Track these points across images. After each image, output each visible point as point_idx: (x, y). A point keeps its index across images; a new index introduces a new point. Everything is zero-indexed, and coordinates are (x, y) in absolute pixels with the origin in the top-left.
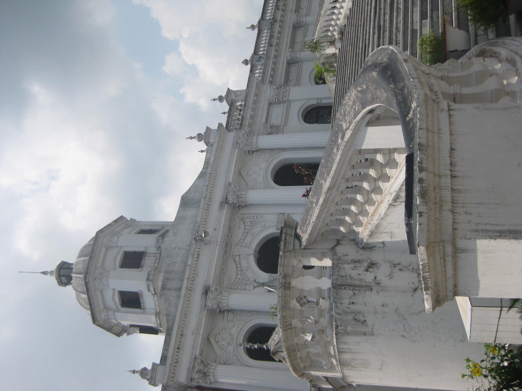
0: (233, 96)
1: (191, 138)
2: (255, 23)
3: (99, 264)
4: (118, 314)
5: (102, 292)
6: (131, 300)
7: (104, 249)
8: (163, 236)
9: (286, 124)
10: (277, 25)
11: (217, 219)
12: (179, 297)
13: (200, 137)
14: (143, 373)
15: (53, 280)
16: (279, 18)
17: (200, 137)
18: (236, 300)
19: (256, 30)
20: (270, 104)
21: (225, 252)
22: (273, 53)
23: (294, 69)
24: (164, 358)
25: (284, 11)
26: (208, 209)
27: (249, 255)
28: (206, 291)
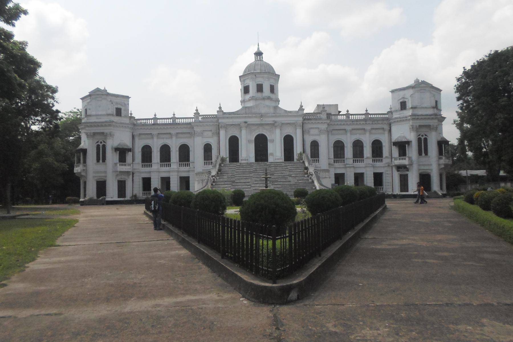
8: (269, 98)
10: (364, 122)
11: (270, 120)
12: (244, 114)
13: (302, 106)
14: (220, 108)
15: (255, 50)
16: (367, 122)
17: (301, 106)
18: (244, 132)
19: (364, 112)
21: (260, 124)
22: (349, 123)
24: (225, 113)
25: (372, 123)
26: (272, 117)
28: (246, 122)
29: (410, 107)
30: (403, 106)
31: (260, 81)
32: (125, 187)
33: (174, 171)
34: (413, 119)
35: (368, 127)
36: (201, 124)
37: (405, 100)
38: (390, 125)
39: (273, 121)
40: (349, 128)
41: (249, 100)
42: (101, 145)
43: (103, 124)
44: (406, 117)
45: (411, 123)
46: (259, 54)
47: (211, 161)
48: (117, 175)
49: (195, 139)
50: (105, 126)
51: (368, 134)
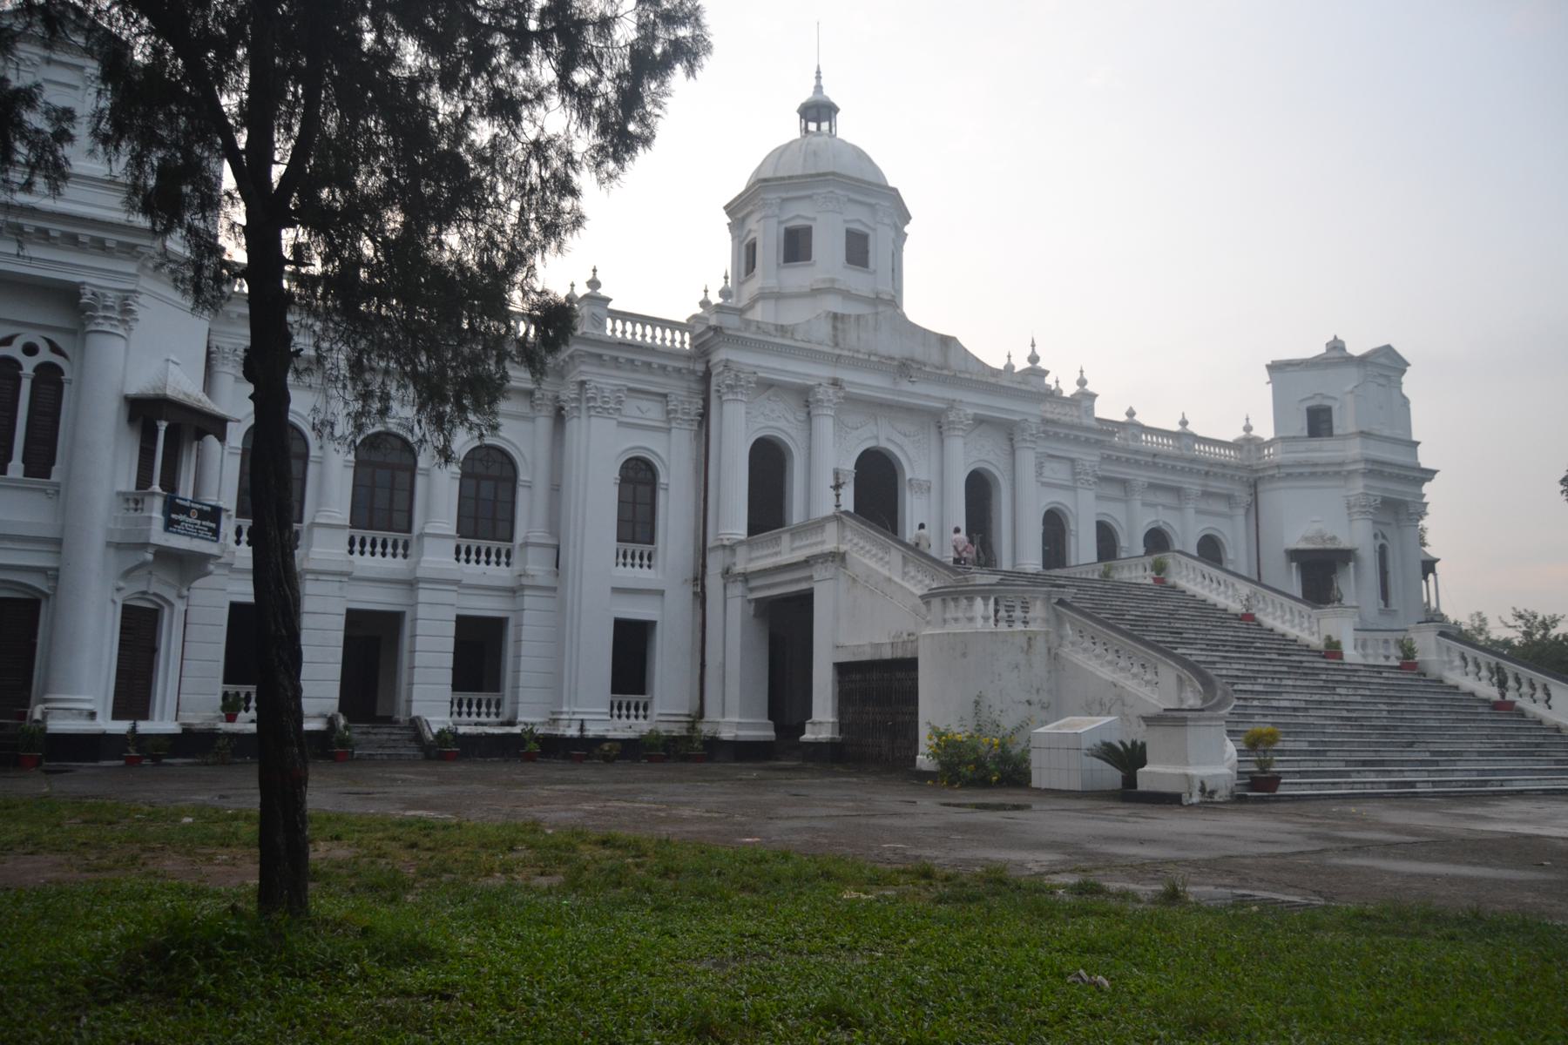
0: (1085, 403)
1: (1033, 346)
2: (1191, 428)
3: (852, 196)
4: (774, 222)
5: (810, 197)
6: (796, 246)
7: (873, 201)
9: (1044, 484)
13: (1034, 359)
17: (1034, 359)
18: (825, 426)
19: (1176, 428)
20: (1072, 460)
23: (1114, 491)
27: (877, 438)
28: (835, 383)
29: (1352, 429)
30: (1319, 422)
31: (858, 217)
32: (154, 650)
33: (439, 582)
34: (1370, 473)
35: (1193, 485)
36: (624, 355)
37: (1327, 403)
38: (1254, 487)
39: (943, 399)
40: (1141, 477)
41: (815, 292)
42: (29, 365)
43: (85, 234)
44: (1341, 464)
45: (1358, 486)
46: (818, 111)
47: (647, 548)
48: (127, 574)
49: (574, 427)
50: (100, 247)
51: (1190, 512)
